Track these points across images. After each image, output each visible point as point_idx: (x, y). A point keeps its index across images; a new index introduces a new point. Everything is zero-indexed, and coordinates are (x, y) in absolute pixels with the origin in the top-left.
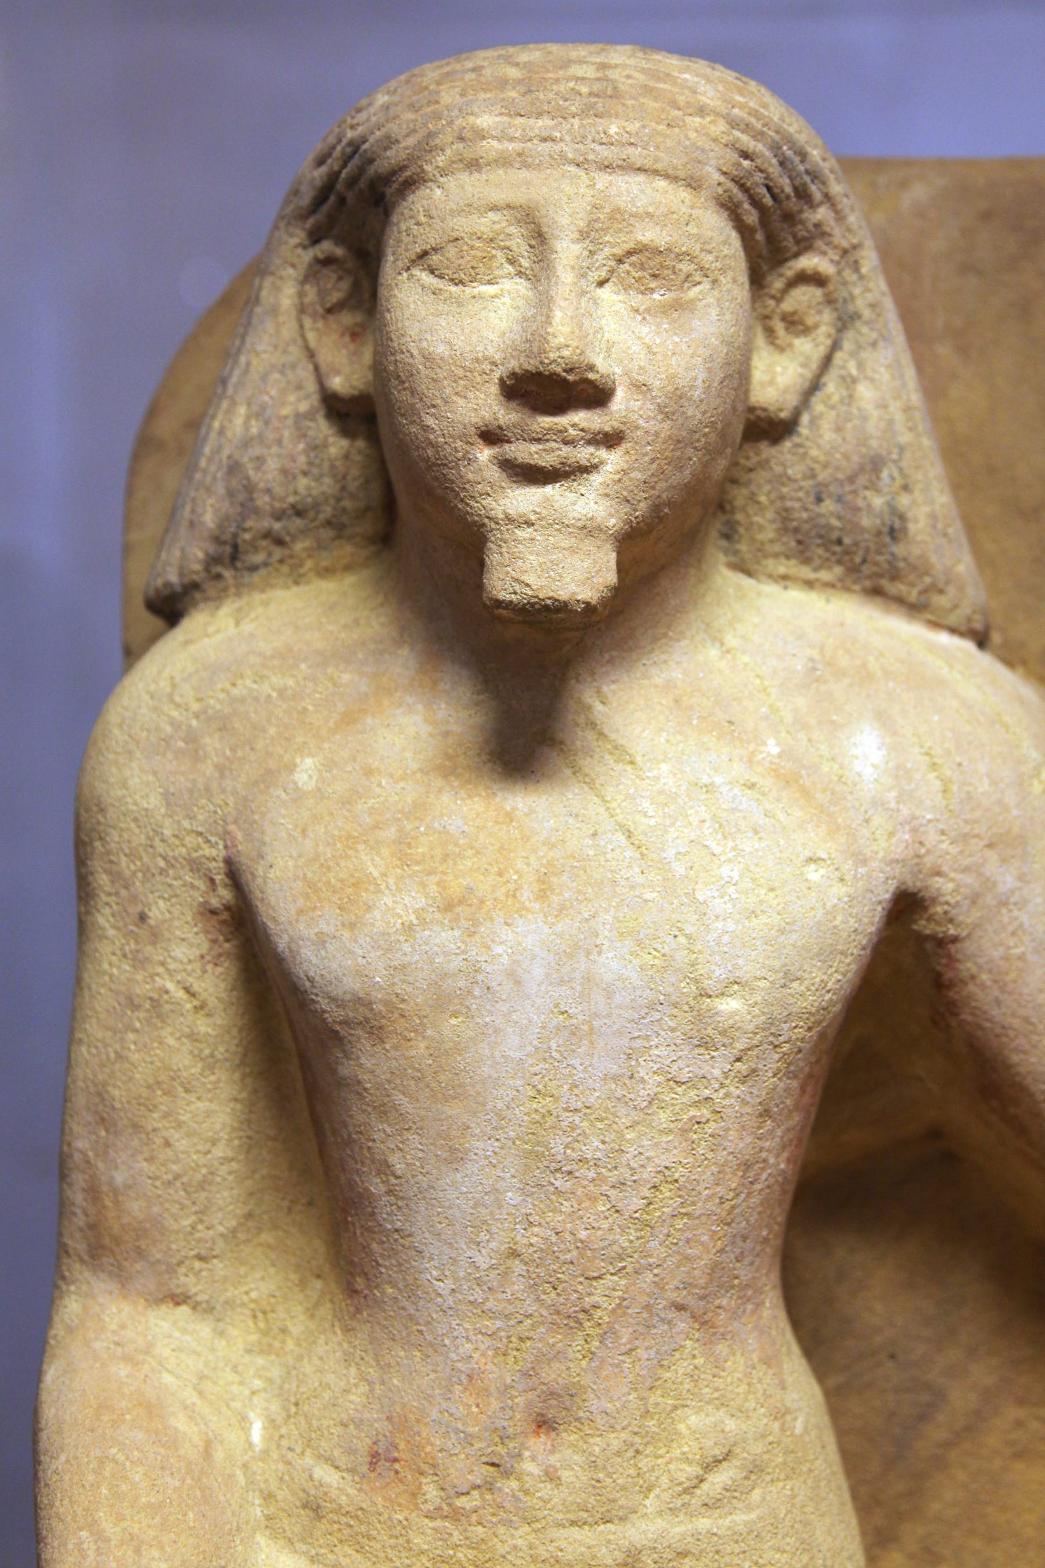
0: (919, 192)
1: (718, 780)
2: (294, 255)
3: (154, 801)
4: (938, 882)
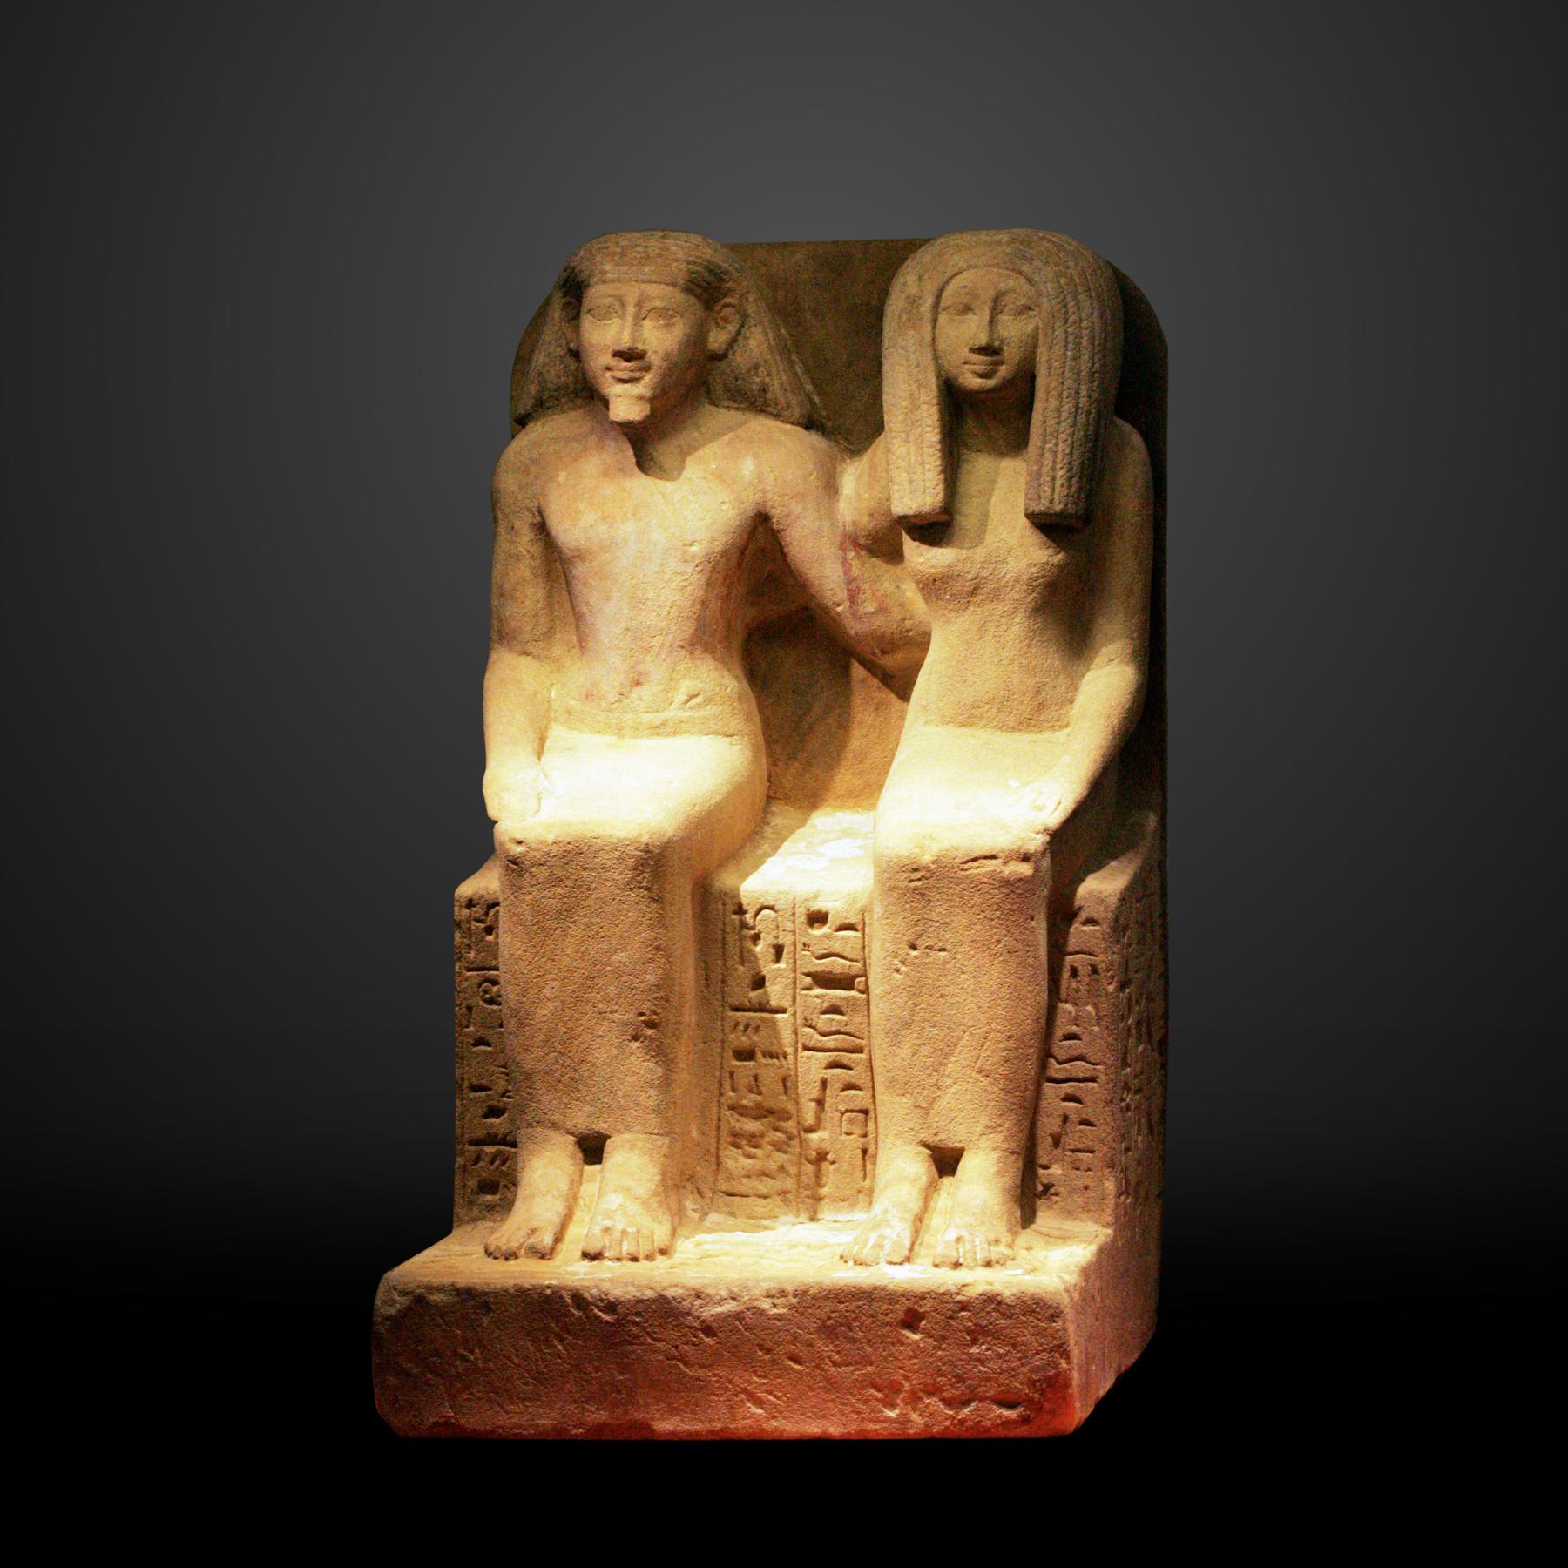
0: (800, 256)
3: (514, 488)
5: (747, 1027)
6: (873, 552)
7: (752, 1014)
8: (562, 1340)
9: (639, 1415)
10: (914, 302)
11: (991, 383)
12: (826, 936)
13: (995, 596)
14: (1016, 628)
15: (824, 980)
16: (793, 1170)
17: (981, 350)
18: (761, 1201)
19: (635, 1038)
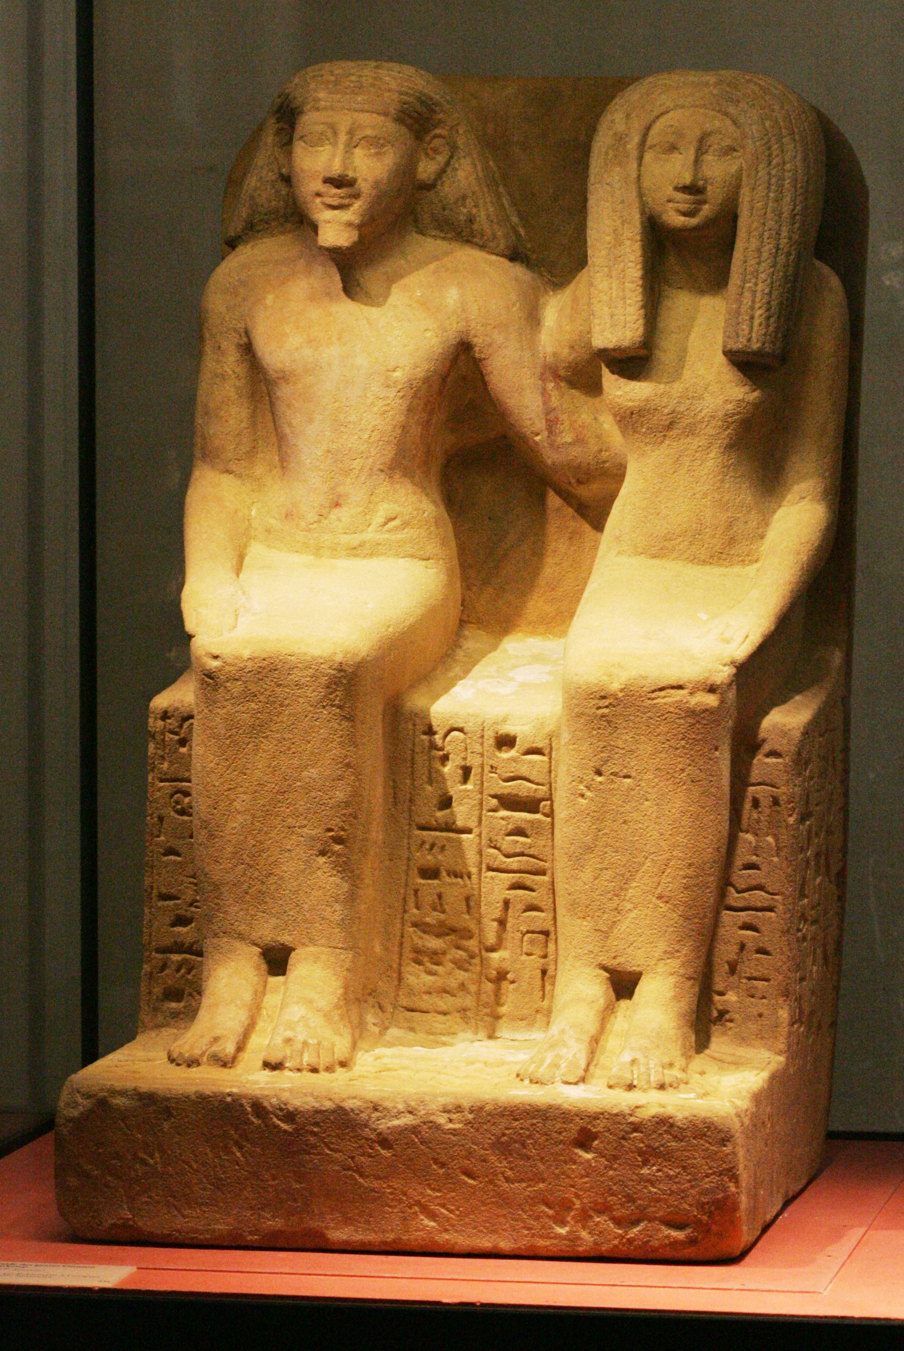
1: (398, 303)
2: (272, 126)
4: (476, 340)
5: (432, 846)
6: (572, 384)
7: (438, 834)
8: (240, 1148)
9: (314, 1224)
10: (620, 139)
11: (694, 221)
12: (514, 760)
13: (691, 431)
14: (710, 463)
15: (510, 802)
16: (473, 988)
17: (685, 189)
18: (441, 1018)
19: (322, 853)
